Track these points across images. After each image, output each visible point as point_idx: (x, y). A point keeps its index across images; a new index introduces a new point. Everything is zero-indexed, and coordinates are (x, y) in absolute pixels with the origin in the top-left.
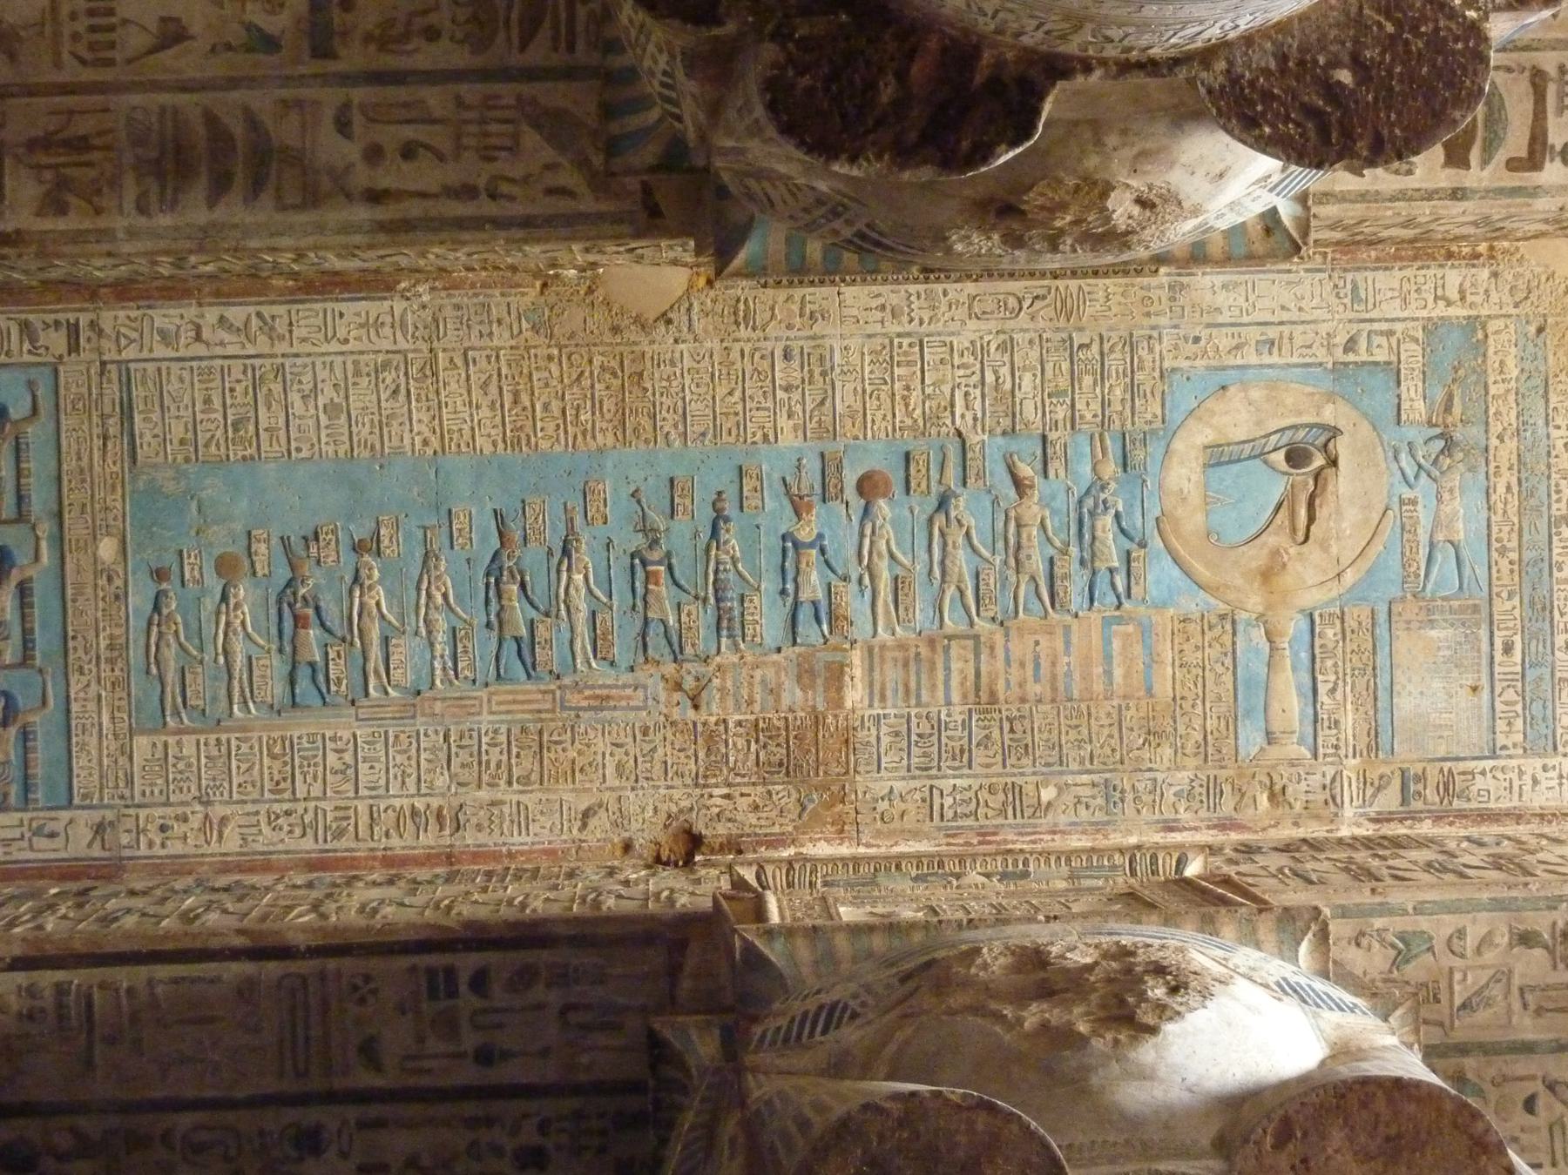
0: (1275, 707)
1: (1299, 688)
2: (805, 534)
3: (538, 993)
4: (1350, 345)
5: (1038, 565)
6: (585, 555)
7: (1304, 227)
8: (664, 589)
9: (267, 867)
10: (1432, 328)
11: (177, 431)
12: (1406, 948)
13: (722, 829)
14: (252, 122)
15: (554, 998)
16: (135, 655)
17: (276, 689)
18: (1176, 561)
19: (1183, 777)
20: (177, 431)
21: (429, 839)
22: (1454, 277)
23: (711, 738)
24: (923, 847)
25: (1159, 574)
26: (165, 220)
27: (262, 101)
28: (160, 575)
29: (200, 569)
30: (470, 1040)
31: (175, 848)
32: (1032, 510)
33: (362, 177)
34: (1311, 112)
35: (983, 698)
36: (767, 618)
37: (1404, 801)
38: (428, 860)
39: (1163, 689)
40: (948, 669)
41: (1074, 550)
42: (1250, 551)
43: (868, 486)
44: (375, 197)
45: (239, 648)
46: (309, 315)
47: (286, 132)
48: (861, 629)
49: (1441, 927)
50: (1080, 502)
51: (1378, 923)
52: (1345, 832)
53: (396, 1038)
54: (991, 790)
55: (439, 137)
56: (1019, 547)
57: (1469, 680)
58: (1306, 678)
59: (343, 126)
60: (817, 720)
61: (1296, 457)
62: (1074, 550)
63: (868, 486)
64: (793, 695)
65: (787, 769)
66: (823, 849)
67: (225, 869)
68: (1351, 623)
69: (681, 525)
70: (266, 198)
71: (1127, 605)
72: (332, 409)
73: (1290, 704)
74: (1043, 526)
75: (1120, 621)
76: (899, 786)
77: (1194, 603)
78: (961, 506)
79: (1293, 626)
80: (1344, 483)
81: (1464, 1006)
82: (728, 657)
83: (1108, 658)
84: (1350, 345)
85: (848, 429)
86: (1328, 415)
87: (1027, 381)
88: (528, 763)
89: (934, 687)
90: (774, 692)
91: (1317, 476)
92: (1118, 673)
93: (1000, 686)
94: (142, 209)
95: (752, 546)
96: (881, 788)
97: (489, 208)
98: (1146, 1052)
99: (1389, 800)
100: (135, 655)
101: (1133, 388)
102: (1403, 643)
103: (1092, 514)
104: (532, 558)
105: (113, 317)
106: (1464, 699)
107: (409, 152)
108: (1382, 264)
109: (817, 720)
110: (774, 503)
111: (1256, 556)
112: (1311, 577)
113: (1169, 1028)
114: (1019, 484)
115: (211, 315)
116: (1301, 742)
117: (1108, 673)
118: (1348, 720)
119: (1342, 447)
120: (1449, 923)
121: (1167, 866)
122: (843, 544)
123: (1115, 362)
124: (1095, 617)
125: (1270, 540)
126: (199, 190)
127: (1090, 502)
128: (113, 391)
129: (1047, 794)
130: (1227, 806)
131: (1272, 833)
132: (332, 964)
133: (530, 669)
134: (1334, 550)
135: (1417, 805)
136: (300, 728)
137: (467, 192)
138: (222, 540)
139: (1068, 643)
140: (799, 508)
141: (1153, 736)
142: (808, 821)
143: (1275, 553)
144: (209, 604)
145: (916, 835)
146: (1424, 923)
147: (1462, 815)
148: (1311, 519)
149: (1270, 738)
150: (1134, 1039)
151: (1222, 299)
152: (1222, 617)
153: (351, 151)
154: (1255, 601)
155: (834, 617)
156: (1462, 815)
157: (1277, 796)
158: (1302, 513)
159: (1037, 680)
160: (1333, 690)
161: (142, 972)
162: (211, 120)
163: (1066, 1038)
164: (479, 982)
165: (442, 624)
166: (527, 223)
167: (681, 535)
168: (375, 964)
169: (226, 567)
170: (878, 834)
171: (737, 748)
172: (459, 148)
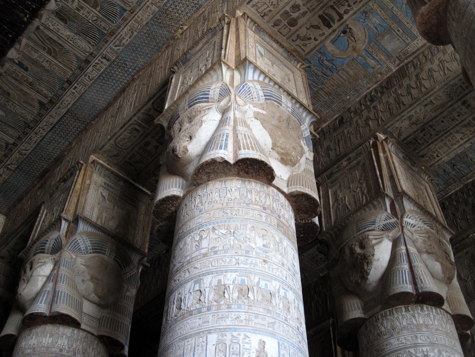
0: (371, 64)
1: (372, 59)
5: (320, 74)
12: (410, 118)
18: (340, 58)
19: (365, 82)
24: (337, 115)
35: (328, 94)
37: (400, 60)
40: (321, 95)
41: (324, 69)
42: (349, 49)
49: (413, 113)
50: (319, 62)
51: (403, 118)
52: (394, 70)
54: (340, 103)
56: (316, 74)
57: (396, 39)
58: (371, 57)
61: (344, 32)
62: (324, 69)
66: (324, 126)
68: (372, 46)
71: (338, 69)
73: (372, 62)
74: (317, 69)
75: (339, 71)
76: (327, 111)
79: (364, 53)
80: (354, 30)
81: (424, 118)
83: (341, 77)
89: (321, 98)
91: (350, 32)
92: (344, 77)
93: (330, 91)
96: (325, 113)
98: (368, 282)
99: (397, 62)
102: (382, 43)
103: (322, 62)
111: (350, 49)
112: (361, 45)
113: (369, 277)
116: (378, 65)
117: (343, 78)
118: (383, 57)
124: (335, 74)
125: (351, 45)
127: (320, 61)
129: (348, 97)
130: (374, 80)
131: (384, 78)
134: (361, 39)
135: (402, 60)
139: (334, 79)
141: (356, 80)
143: (353, 47)
145: (335, 115)
146: (410, 114)
147: (410, 56)
148: (354, 38)
149: (373, 68)
150: (366, 281)
152: (353, 60)
154: (356, 55)
156: (410, 56)
157: (381, 74)
158: (352, 38)
159: (334, 86)
160: (377, 56)
170: (330, 118)
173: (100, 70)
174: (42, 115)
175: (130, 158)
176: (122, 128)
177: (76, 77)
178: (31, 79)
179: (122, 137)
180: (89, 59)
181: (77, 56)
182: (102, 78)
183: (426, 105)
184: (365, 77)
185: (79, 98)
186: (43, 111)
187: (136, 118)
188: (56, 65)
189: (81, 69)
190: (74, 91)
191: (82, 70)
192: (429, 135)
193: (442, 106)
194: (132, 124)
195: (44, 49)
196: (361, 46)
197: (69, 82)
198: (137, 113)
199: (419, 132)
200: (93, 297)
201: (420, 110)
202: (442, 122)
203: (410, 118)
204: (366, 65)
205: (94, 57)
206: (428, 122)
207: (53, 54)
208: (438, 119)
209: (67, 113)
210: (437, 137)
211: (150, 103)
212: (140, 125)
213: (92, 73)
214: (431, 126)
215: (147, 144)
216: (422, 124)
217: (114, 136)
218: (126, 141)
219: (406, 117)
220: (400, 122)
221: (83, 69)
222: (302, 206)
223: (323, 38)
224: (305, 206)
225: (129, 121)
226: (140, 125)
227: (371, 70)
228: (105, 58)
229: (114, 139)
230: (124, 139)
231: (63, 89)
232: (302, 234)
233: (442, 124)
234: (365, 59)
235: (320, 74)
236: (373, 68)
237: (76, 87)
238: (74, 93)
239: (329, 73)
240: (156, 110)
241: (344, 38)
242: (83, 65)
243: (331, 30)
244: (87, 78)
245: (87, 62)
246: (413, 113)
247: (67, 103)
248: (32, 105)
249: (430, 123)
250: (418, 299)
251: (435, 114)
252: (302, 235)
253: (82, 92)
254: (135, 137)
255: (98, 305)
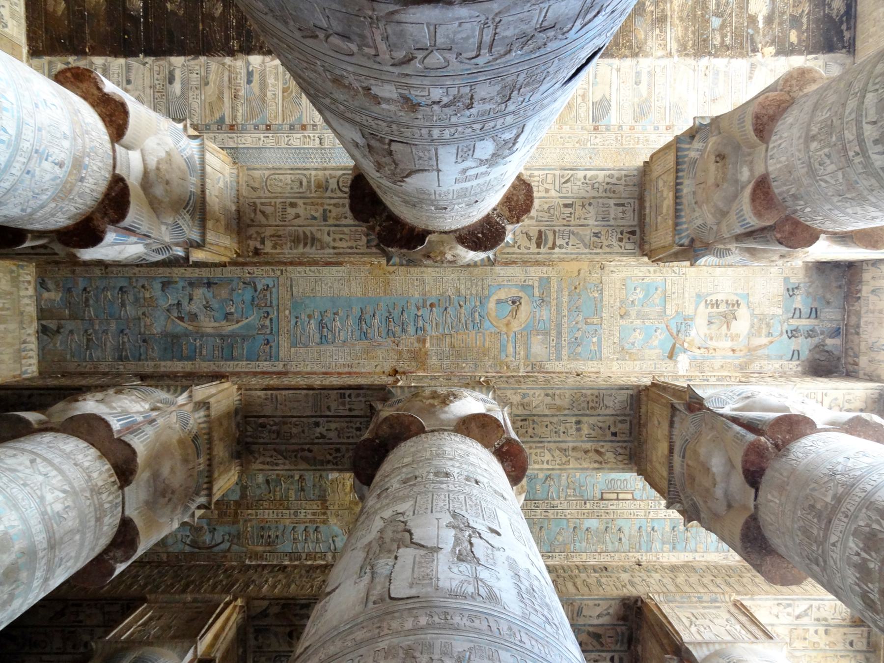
2: (419, 314)
3: (360, 398)
4: (525, 281)
5: (463, 321)
6: (377, 316)
7: (495, 260)
8: (392, 323)
9: (315, 374)
10: (541, 279)
11: (301, 290)
12: (524, 396)
13: (402, 370)
14: (312, 233)
15: (363, 399)
16: (292, 332)
17: (318, 340)
20: (301, 290)
21: (346, 369)
22: (545, 269)
23: (400, 353)
25: (486, 324)
26: (295, 251)
27: (314, 229)
28: (297, 318)
29: (304, 317)
30: (347, 407)
31: (298, 369)
32: (463, 311)
33: (332, 244)
34: (474, 242)
35: (452, 346)
36: (411, 329)
38: (346, 373)
39: (487, 346)
43: (432, 305)
44: (334, 248)
45: (311, 332)
46: (326, 270)
47: (318, 235)
48: (429, 333)
49: (531, 392)
53: (334, 406)
55: (347, 237)
59: (329, 234)
60: (420, 349)
61: (514, 302)
63: (432, 305)
64: (416, 345)
65: (414, 359)
66: (421, 374)
67: (308, 374)
69: (396, 311)
70: (314, 248)
72: (330, 287)
73: (511, 350)
77: (493, 330)
78: (449, 310)
79: (512, 335)
80: (523, 308)
82: (404, 337)
84: (525, 281)
85: (429, 294)
86: (520, 294)
87: (463, 286)
88: (365, 356)
90: (412, 344)
94: (291, 249)
95: (409, 316)
97: (355, 250)
98: (446, 409)
99: (529, 369)
100: (292, 332)
101: (483, 288)
104: (367, 317)
105: (289, 268)
106: (544, 349)
107: (341, 240)
108: (532, 266)
109: (420, 349)
110: (413, 308)
111: (505, 321)
114: (460, 306)
115: (308, 268)
118: (522, 353)
119: (522, 301)
120: (532, 391)
121: (477, 379)
122: (427, 318)
123: (479, 283)
125: (508, 318)
126: (301, 245)
128: (289, 282)
129: (464, 365)
130: (498, 369)
132: (323, 391)
133: (366, 338)
136: (323, 348)
137: (351, 248)
138: (308, 311)
140: (418, 309)
141: (485, 355)
142: (418, 369)
144: (306, 323)
146: (528, 391)
149: (507, 356)
151: (501, 272)
153: (330, 239)
154: (504, 330)
155: (423, 329)
157: (508, 367)
161: (287, 392)
162: (304, 233)
163: (433, 406)
164: (350, 396)
165: (350, 329)
166: (362, 254)
167: (396, 313)
168: (330, 392)
169: (310, 317)
171: (406, 355)
172: (350, 239)
173: (304, 143)
174: (209, 129)
175: (262, 204)
176: (292, 169)
177: (280, 129)
178: (242, 93)
179: (281, 177)
180: (308, 127)
181: (301, 115)
182: (298, 151)
183: (547, 395)
184: (494, 358)
185: (259, 148)
186: (215, 127)
187: (313, 173)
188: (277, 104)
189: (292, 128)
190: (262, 139)
191: (291, 129)
192: (524, 431)
193: (559, 409)
194: (305, 175)
195: (284, 84)
196: (516, 326)
197: (268, 128)
198: (320, 169)
199: (519, 418)
200: (152, 163)
201: (539, 395)
202: (547, 426)
203: (524, 396)
204: (503, 348)
205: (314, 130)
206: (534, 415)
207: (285, 94)
208: (545, 419)
209: (232, 148)
210: (529, 439)
211: (341, 172)
212: (309, 182)
213: (296, 140)
214: (533, 421)
215: (293, 205)
216: (528, 413)
217: (276, 169)
218: (280, 184)
219: (523, 391)
220: (513, 392)
221: (293, 129)
222: (515, 199)
223: (526, 251)
224: (517, 201)
225: (305, 169)
226: (309, 182)
227: (503, 356)
228: (321, 139)
229: (272, 172)
230: (281, 180)
231: (256, 127)
232: (482, 233)
233: (545, 428)
234: (508, 342)
235: (463, 321)
236: (507, 356)
237: (268, 137)
238: (260, 139)
239: (470, 326)
240: (338, 182)
241: (509, 307)
242: (297, 126)
243: (537, 250)
244: (287, 139)
245: (304, 127)
246: (531, 392)
247: (243, 141)
248: (212, 112)
249: (535, 418)
250: (502, 446)
251: (547, 412)
252: (480, 235)
253: (268, 146)
254: (292, 188)
255: (146, 173)
